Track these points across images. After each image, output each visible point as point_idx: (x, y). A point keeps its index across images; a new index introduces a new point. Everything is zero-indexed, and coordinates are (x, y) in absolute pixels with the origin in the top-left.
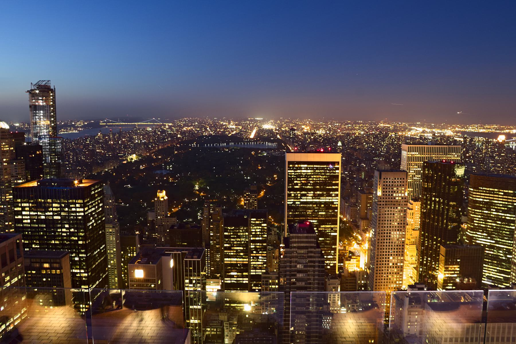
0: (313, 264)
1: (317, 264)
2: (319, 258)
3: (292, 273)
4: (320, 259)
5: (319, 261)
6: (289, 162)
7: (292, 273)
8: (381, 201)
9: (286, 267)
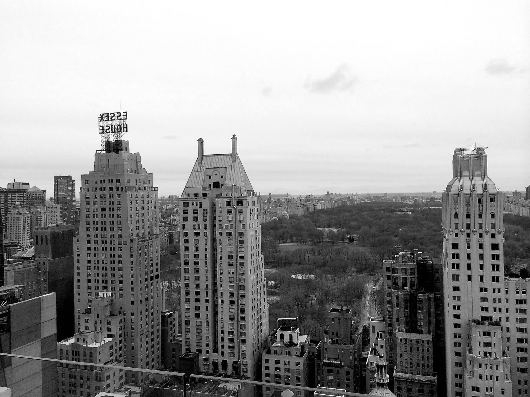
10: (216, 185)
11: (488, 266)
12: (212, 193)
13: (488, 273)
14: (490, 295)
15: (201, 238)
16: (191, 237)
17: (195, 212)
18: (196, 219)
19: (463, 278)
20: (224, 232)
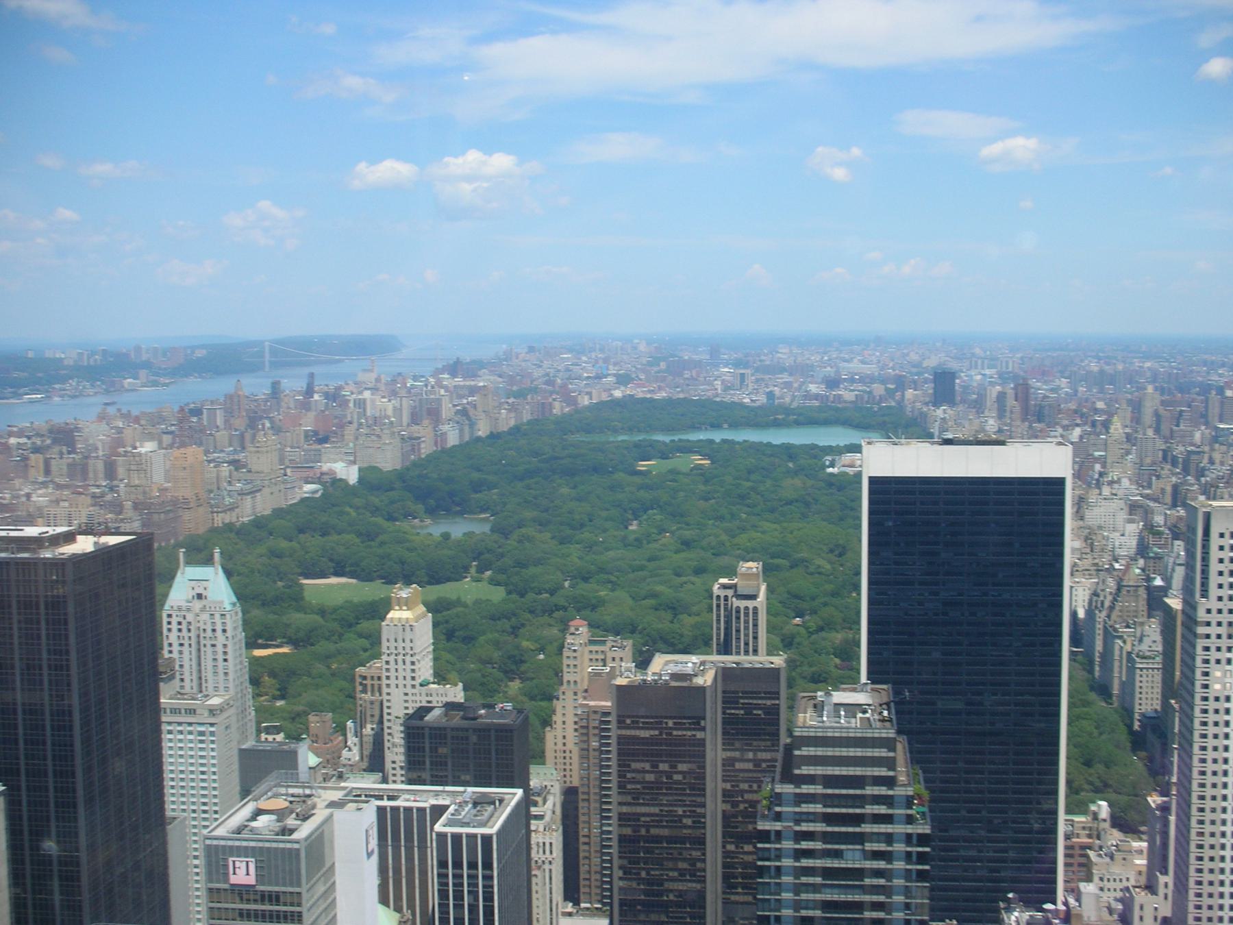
0: (882, 847)
1: (899, 847)
2: (910, 820)
3: (804, 880)
4: (910, 829)
5: (908, 838)
6: (872, 480)
7: (804, 880)
8: (1208, 624)
9: (778, 858)
10: (200, 596)
11: (408, 678)
12: (197, 605)
13: (409, 682)
14: (409, 698)
15: (186, 649)
16: (176, 648)
17: (180, 623)
18: (180, 630)
19: (393, 686)
20: (209, 643)
